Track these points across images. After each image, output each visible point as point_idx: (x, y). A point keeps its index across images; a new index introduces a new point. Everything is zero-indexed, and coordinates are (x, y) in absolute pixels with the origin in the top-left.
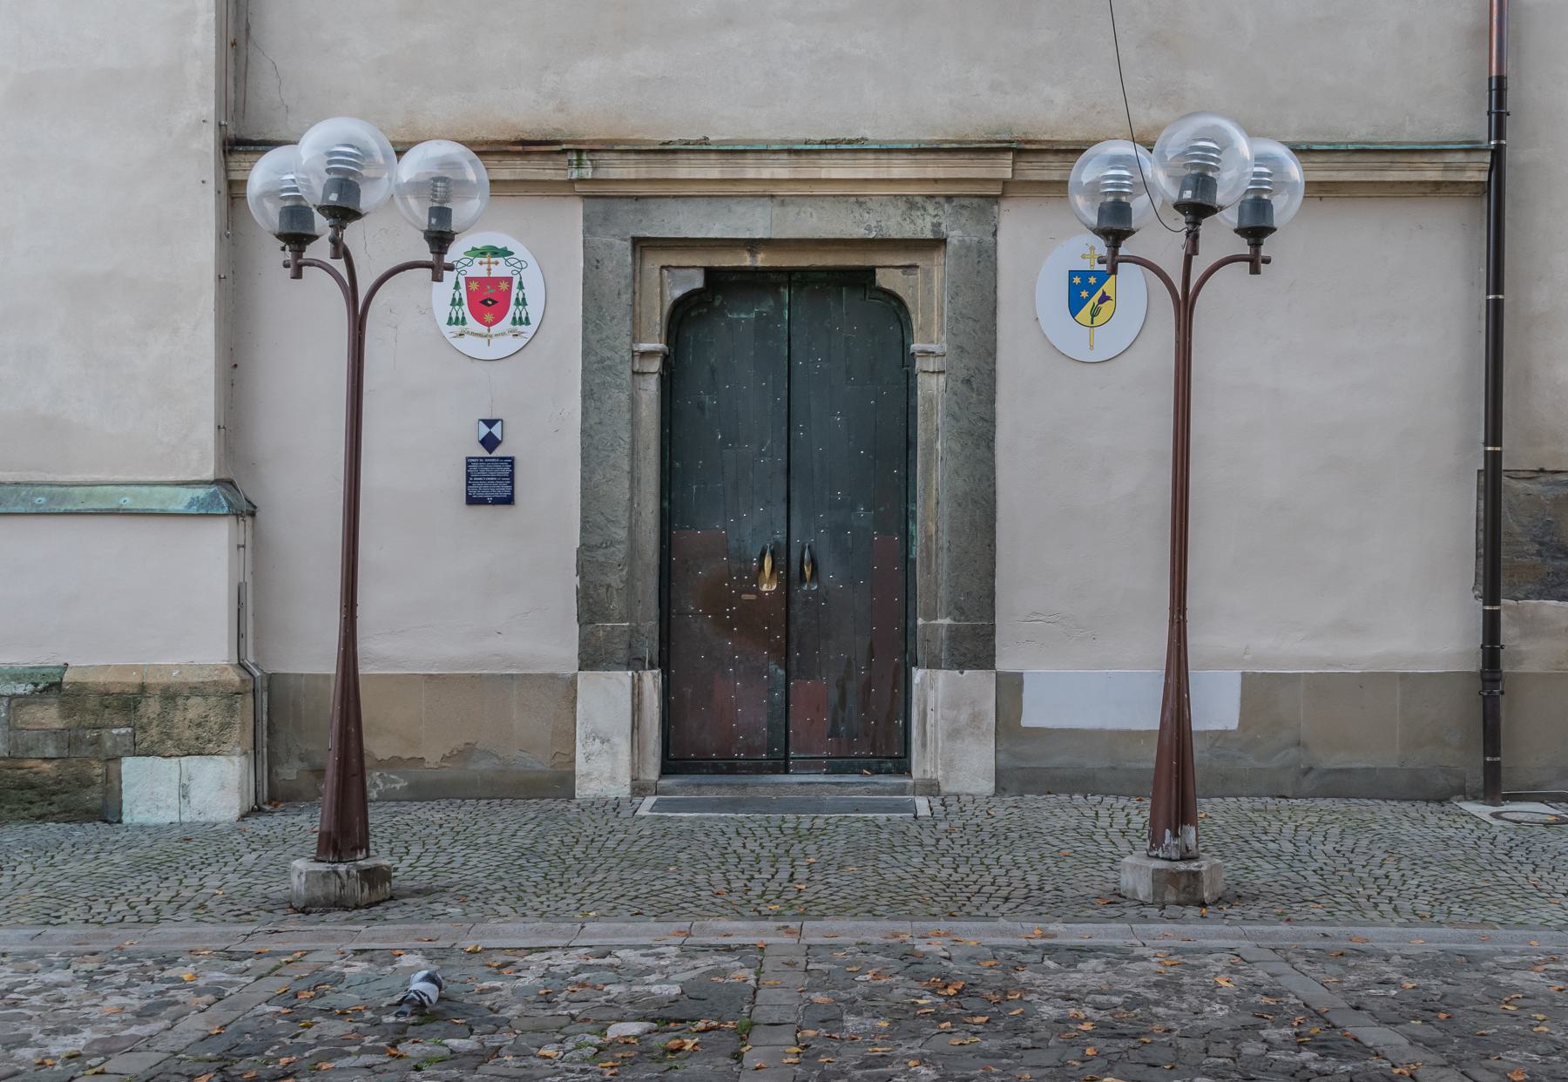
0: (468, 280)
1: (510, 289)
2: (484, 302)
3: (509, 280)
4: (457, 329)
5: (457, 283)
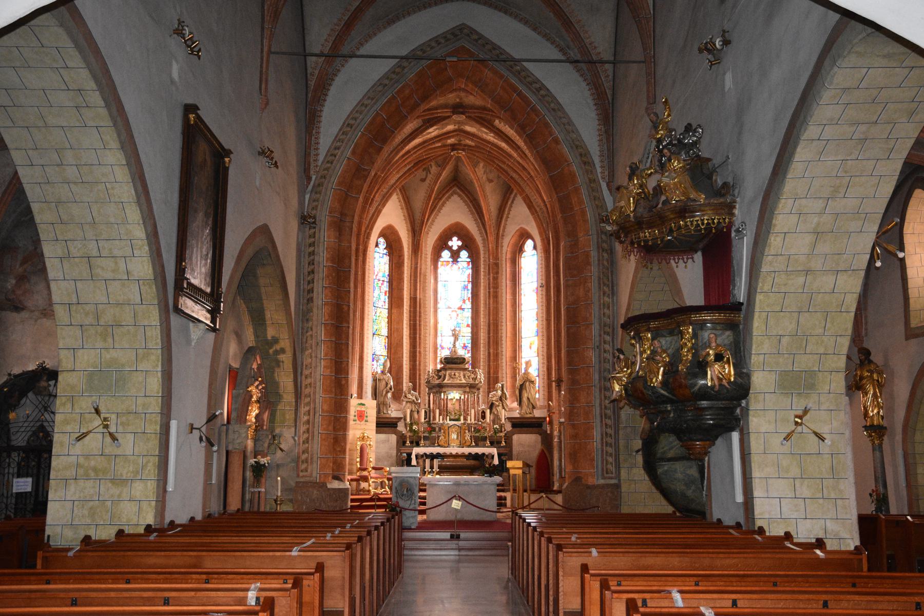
4: (355, 422)
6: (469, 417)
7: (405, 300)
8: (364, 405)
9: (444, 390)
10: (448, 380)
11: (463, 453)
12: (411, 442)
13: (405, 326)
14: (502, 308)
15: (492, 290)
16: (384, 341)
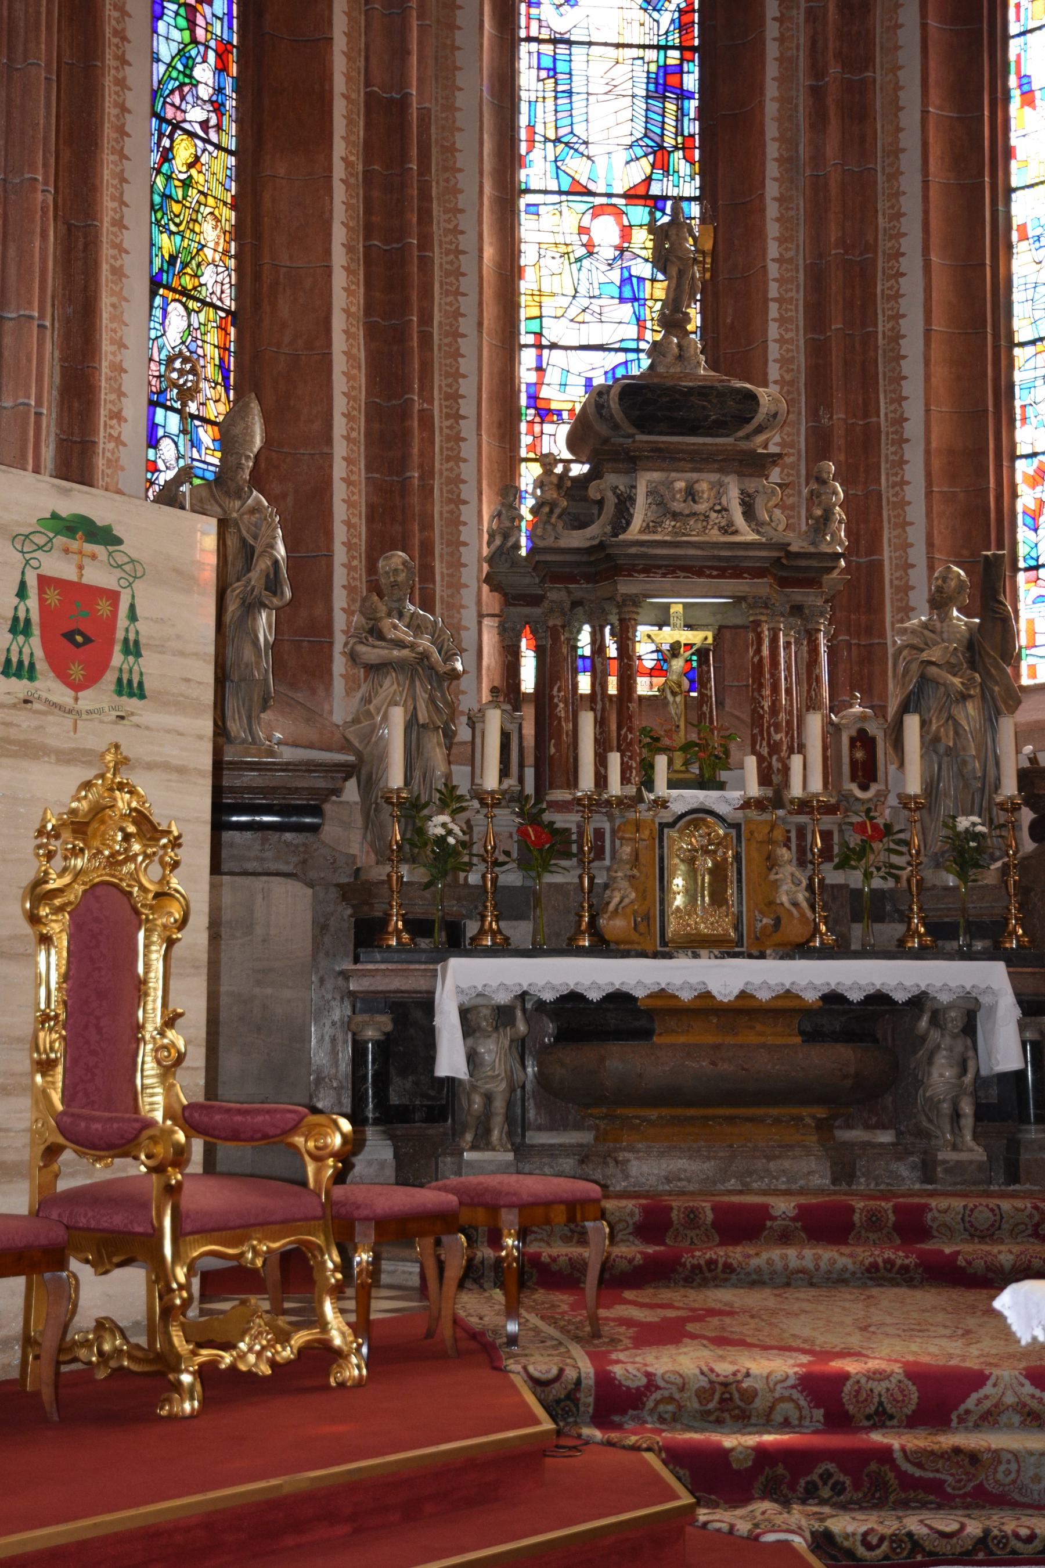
0: (44, 582)
1: (115, 613)
2: (69, 636)
3: (113, 597)
4: (19, 687)
5: (23, 585)
6: (796, 761)
7: (339, 108)
8: (104, 536)
9: (626, 587)
10: (646, 529)
11: (788, 994)
12: (418, 927)
13: (339, 257)
14: (895, 175)
15: (834, 69)
16: (213, 337)
